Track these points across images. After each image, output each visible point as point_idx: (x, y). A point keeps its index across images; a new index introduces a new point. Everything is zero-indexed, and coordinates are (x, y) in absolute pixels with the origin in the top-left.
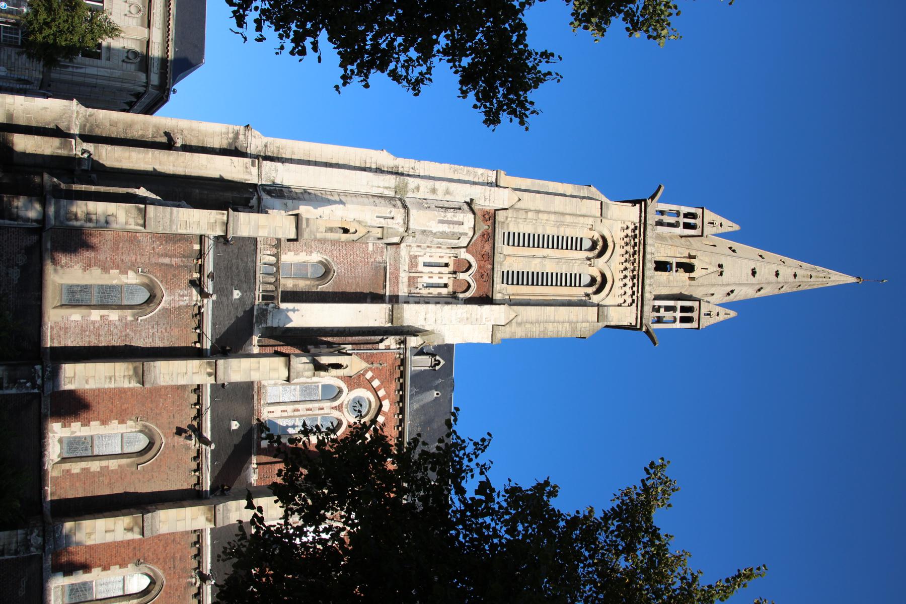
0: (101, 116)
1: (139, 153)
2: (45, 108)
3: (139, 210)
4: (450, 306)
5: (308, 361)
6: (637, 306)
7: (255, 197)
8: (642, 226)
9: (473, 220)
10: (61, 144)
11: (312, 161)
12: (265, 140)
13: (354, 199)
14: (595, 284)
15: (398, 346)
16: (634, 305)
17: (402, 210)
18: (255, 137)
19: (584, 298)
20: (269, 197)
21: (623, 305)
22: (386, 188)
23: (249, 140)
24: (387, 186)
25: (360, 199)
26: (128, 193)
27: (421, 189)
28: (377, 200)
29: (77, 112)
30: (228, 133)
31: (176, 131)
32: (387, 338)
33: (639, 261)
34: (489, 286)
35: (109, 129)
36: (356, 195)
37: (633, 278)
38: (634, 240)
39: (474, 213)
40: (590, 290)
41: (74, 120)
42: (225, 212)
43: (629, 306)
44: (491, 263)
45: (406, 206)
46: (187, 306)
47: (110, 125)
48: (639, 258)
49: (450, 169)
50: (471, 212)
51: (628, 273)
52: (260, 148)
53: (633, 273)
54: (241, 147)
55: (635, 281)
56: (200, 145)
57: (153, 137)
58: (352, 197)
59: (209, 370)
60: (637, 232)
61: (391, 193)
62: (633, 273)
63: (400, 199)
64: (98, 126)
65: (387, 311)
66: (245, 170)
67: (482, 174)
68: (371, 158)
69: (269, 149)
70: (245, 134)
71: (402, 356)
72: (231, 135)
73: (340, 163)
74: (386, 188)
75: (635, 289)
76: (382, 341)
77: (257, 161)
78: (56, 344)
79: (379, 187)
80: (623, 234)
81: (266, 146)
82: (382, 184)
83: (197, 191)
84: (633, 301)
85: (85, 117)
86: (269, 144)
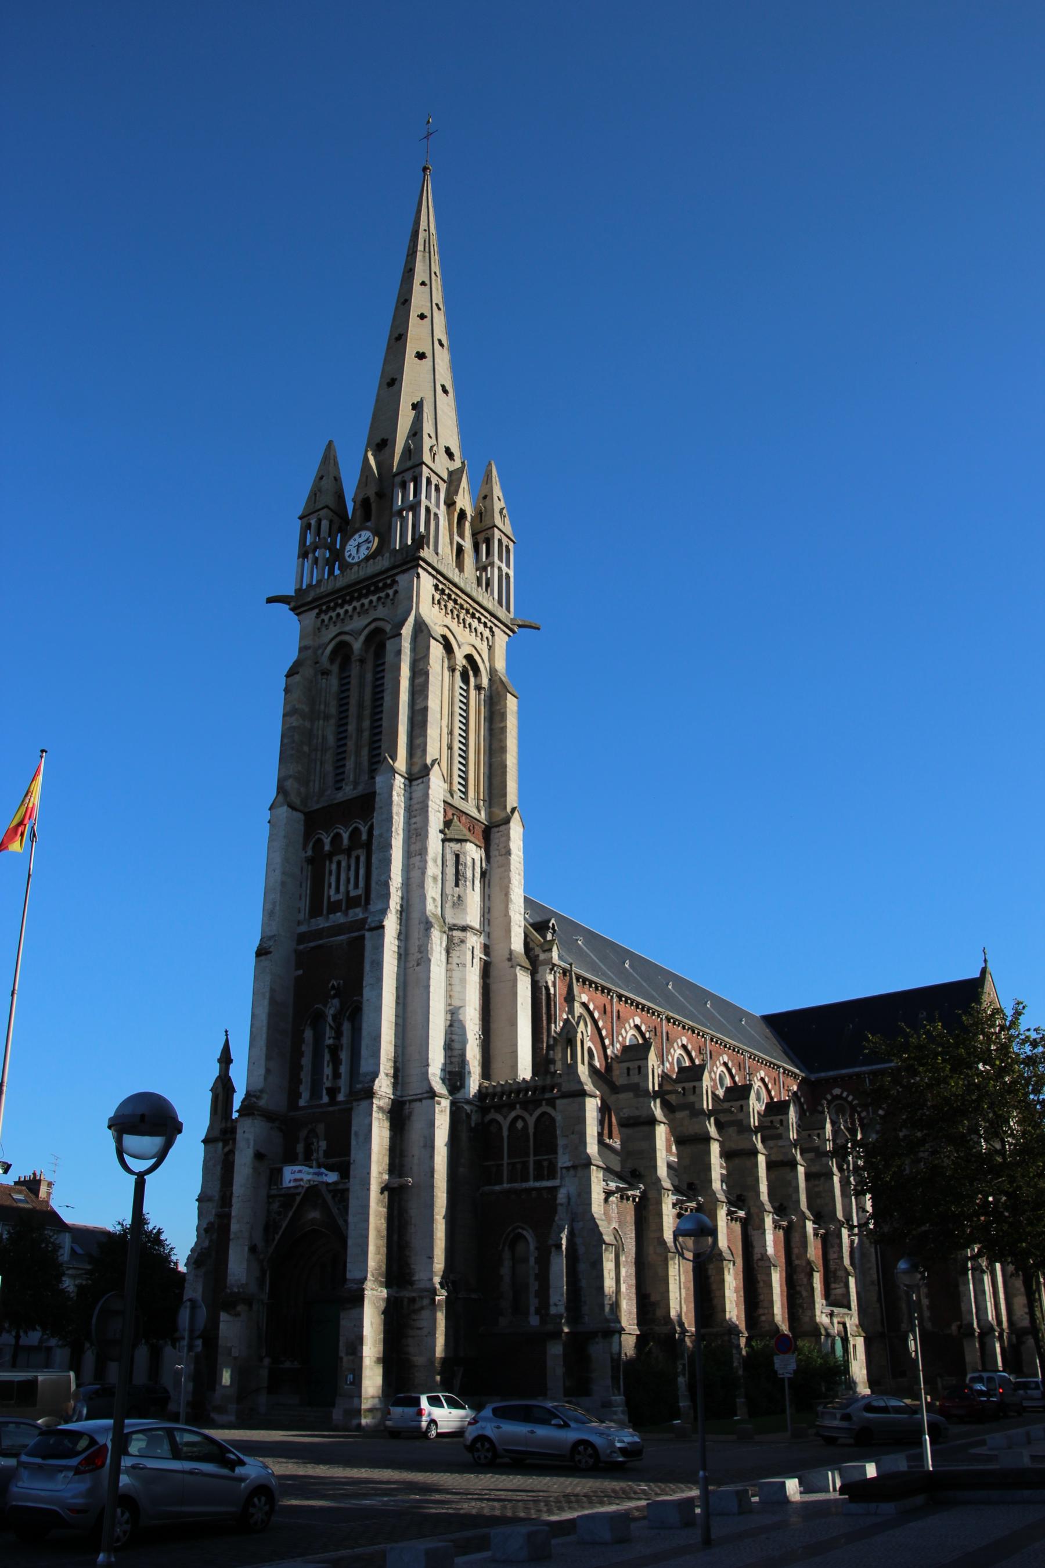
0: (373, 1264)
1: (437, 1229)
2: (372, 1324)
3: (606, 1249)
4: (511, 892)
5: (652, 1103)
6: (496, 626)
7: (466, 1107)
8: (439, 577)
9: (471, 844)
10: (440, 1310)
11: (396, 1021)
12: (382, 1075)
13: (457, 988)
14: (467, 668)
15: (553, 972)
16: (495, 629)
17: (469, 934)
18: (380, 1087)
19: (482, 696)
20: (462, 1091)
21: (490, 644)
22: (441, 943)
23: (384, 1094)
24: (439, 942)
25: (455, 981)
26: (566, 1257)
27: (434, 896)
28: (455, 960)
29: (372, 1289)
30: (379, 1119)
31: (380, 1180)
32: (547, 982)
33: (464, 600)
34: (478, 825)
35: (382, 1255)
36: (449, 984)
37: (473, 616)
38: (445, 595)
39: (466, 841)
40: (472, 680)
41: (379, 1294)
42: (592, 1167)
43: (493, 635)
44: (461, 814)
45: (463, 927)
46: (617, 1206)
47: (379, 1254)
48: (462, 598)
49: (396, 839)
50: (464, 844)
51: (469, 620)
52: (389, 1083)
53: (469, 613)
54: (388, 1105)
55: (477, 615)
56: (388, 1153)
57: (384, 1207)
58: (451, 990)
59: (666, 1196)
60: (441, 586)
61: (445, 937)
62: (469, 613)
63: (451, 929)
64: (380, 1267)
65: (521, 972)
66: (443, 1113)
67: (398, 795)
68: (391, 943)
69: (389, 1072)
70: (379, 1098)
71: (561, 971)
72: (381, 1115)
73: (395, 985)
74: (441, 943)
75: (483, 619)
76: (547, 988)
77: (437, 1098)
78: (635, 1322)
79: (441, 953)
80: (437, 607)
81: (387, 1075)
82: (439, 947)
83: (461, 1170)
84: (491, 629)
85: (374, 1281)
86: (386, 1071)
